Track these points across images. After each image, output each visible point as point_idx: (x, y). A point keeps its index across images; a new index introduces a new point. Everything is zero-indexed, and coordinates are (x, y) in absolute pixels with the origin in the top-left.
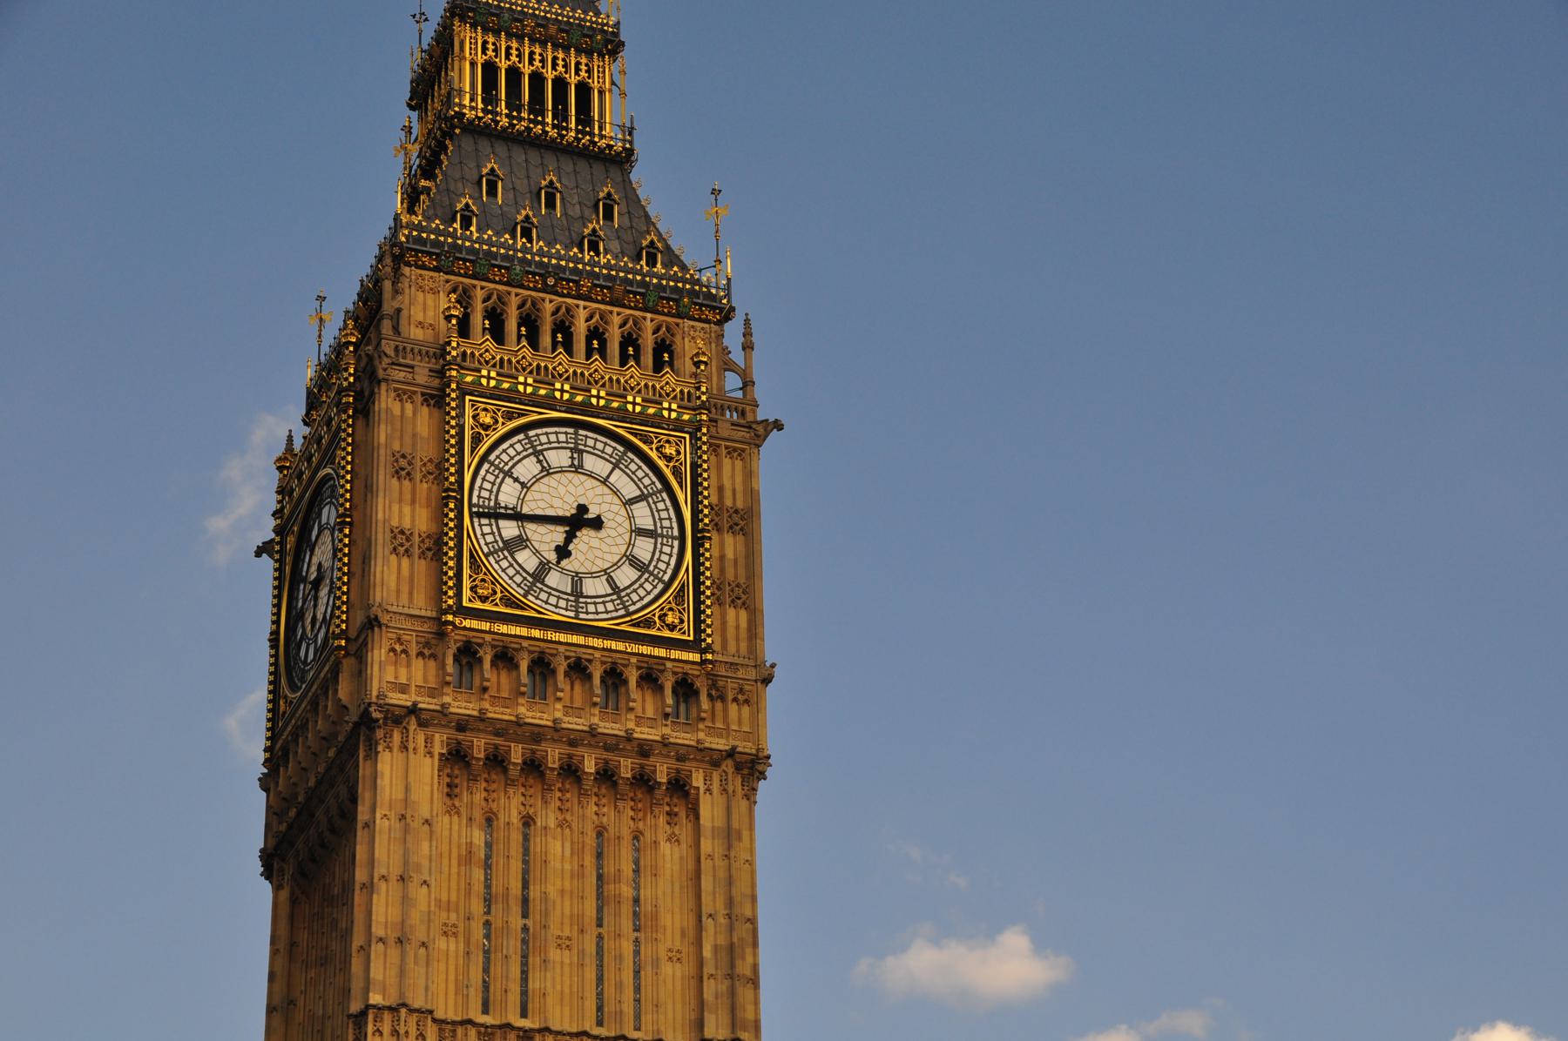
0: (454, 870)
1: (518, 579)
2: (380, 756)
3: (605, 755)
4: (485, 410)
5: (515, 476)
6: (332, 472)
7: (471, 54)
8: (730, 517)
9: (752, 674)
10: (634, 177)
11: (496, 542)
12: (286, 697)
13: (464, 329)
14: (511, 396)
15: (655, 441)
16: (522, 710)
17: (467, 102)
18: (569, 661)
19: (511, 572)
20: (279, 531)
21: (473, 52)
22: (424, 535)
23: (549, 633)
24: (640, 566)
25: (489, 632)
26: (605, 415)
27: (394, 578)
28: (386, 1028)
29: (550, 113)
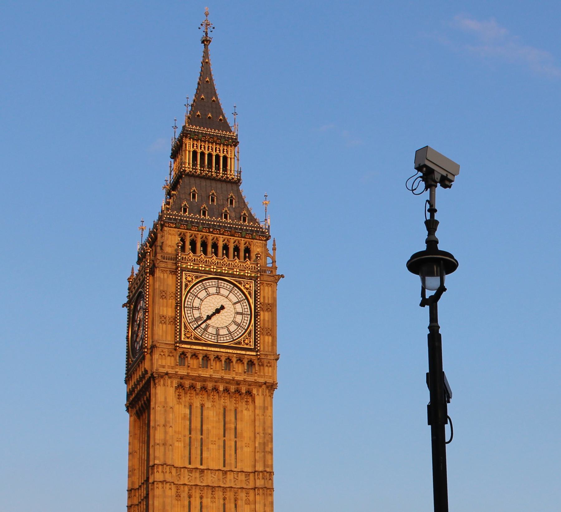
0: (180, 421)
2: (157, 388)
4: (189, 276)
5: (198, 297)
7: (189, 148)
8: (267, 306)
9: (272, 357)
10: (241, 188)
11: (192, 319)
13: (183, 249)
14: (197, 271)
16: (200, 372)
21: (189, 148)
22: (170, 317)
27: (161, 331)
28: (160, 470)
29: (214, 168)
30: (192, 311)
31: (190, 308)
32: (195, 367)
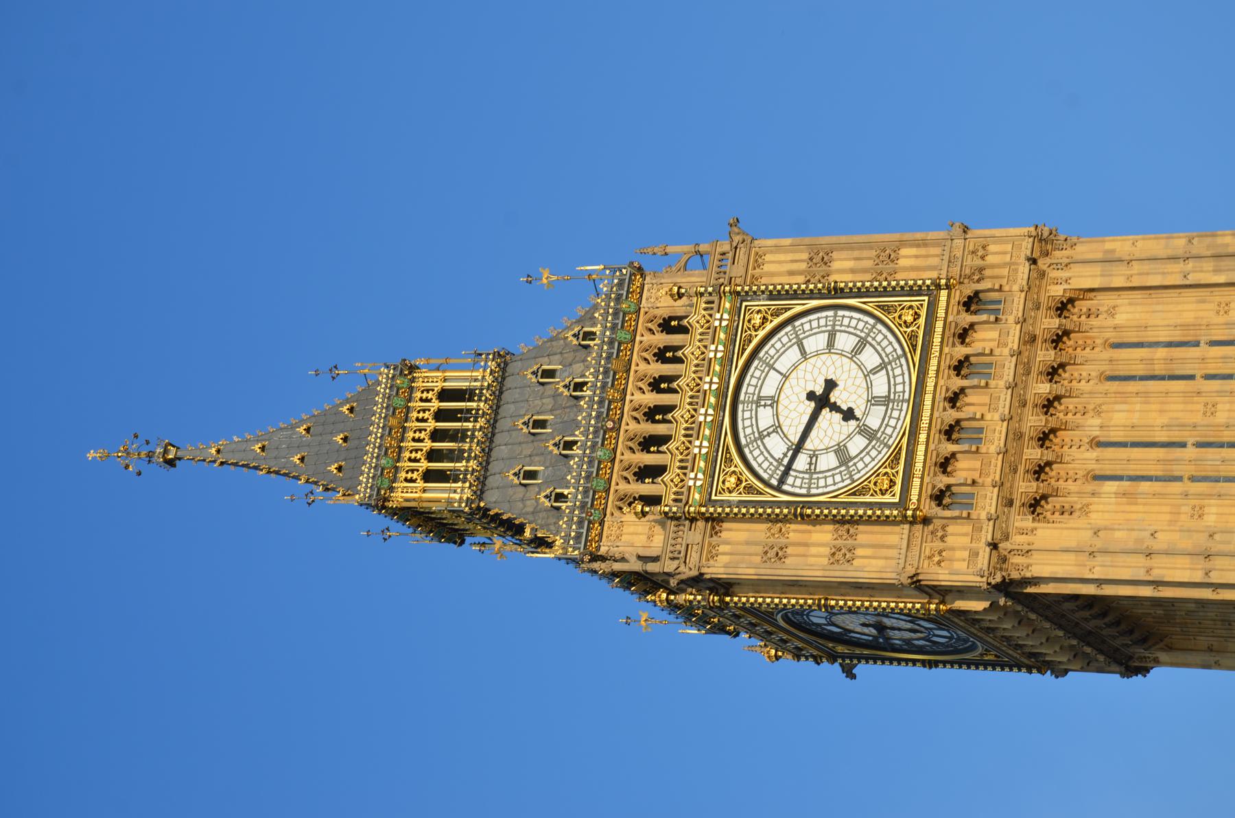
0: (1140, 508)
1: (874, 453)
3: (1034, 374)
4: (724, 482)
5: (782, 456)
6: (780, 615)
7: (416, 492)
11: (841, 472)
12: (982, 655)
13: (654, 500)
14: (712, 461)
15: (749, 332)
16: (993, 449)
17: (457, 496)
18: (948, 408)
19: (867, 459)
20: (833, 658)
23: (922, 425)
24: (861, 345)
25: (922, 478)
26: (727, 377)
27: (874, 562)
29: (465, 424)
30: (820, 472)
31: (811, 479)
32: (977, 464)
